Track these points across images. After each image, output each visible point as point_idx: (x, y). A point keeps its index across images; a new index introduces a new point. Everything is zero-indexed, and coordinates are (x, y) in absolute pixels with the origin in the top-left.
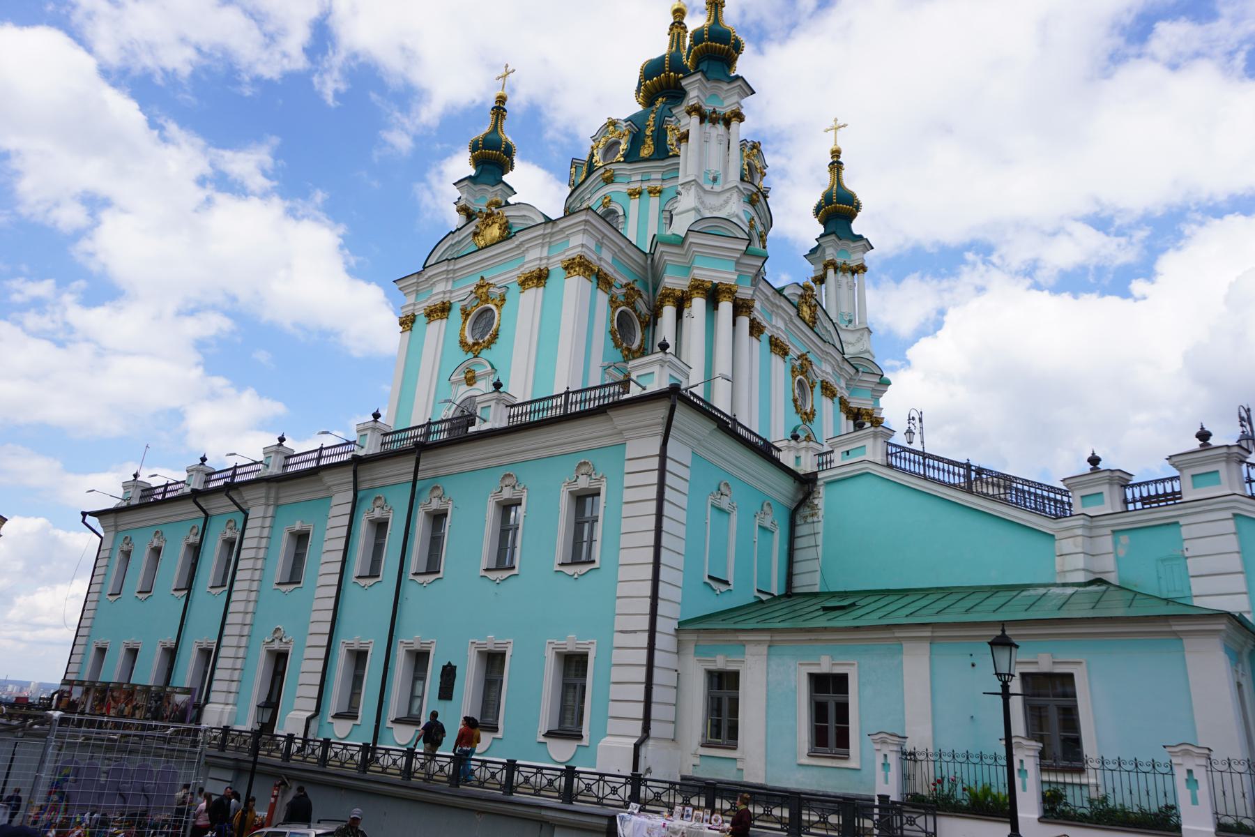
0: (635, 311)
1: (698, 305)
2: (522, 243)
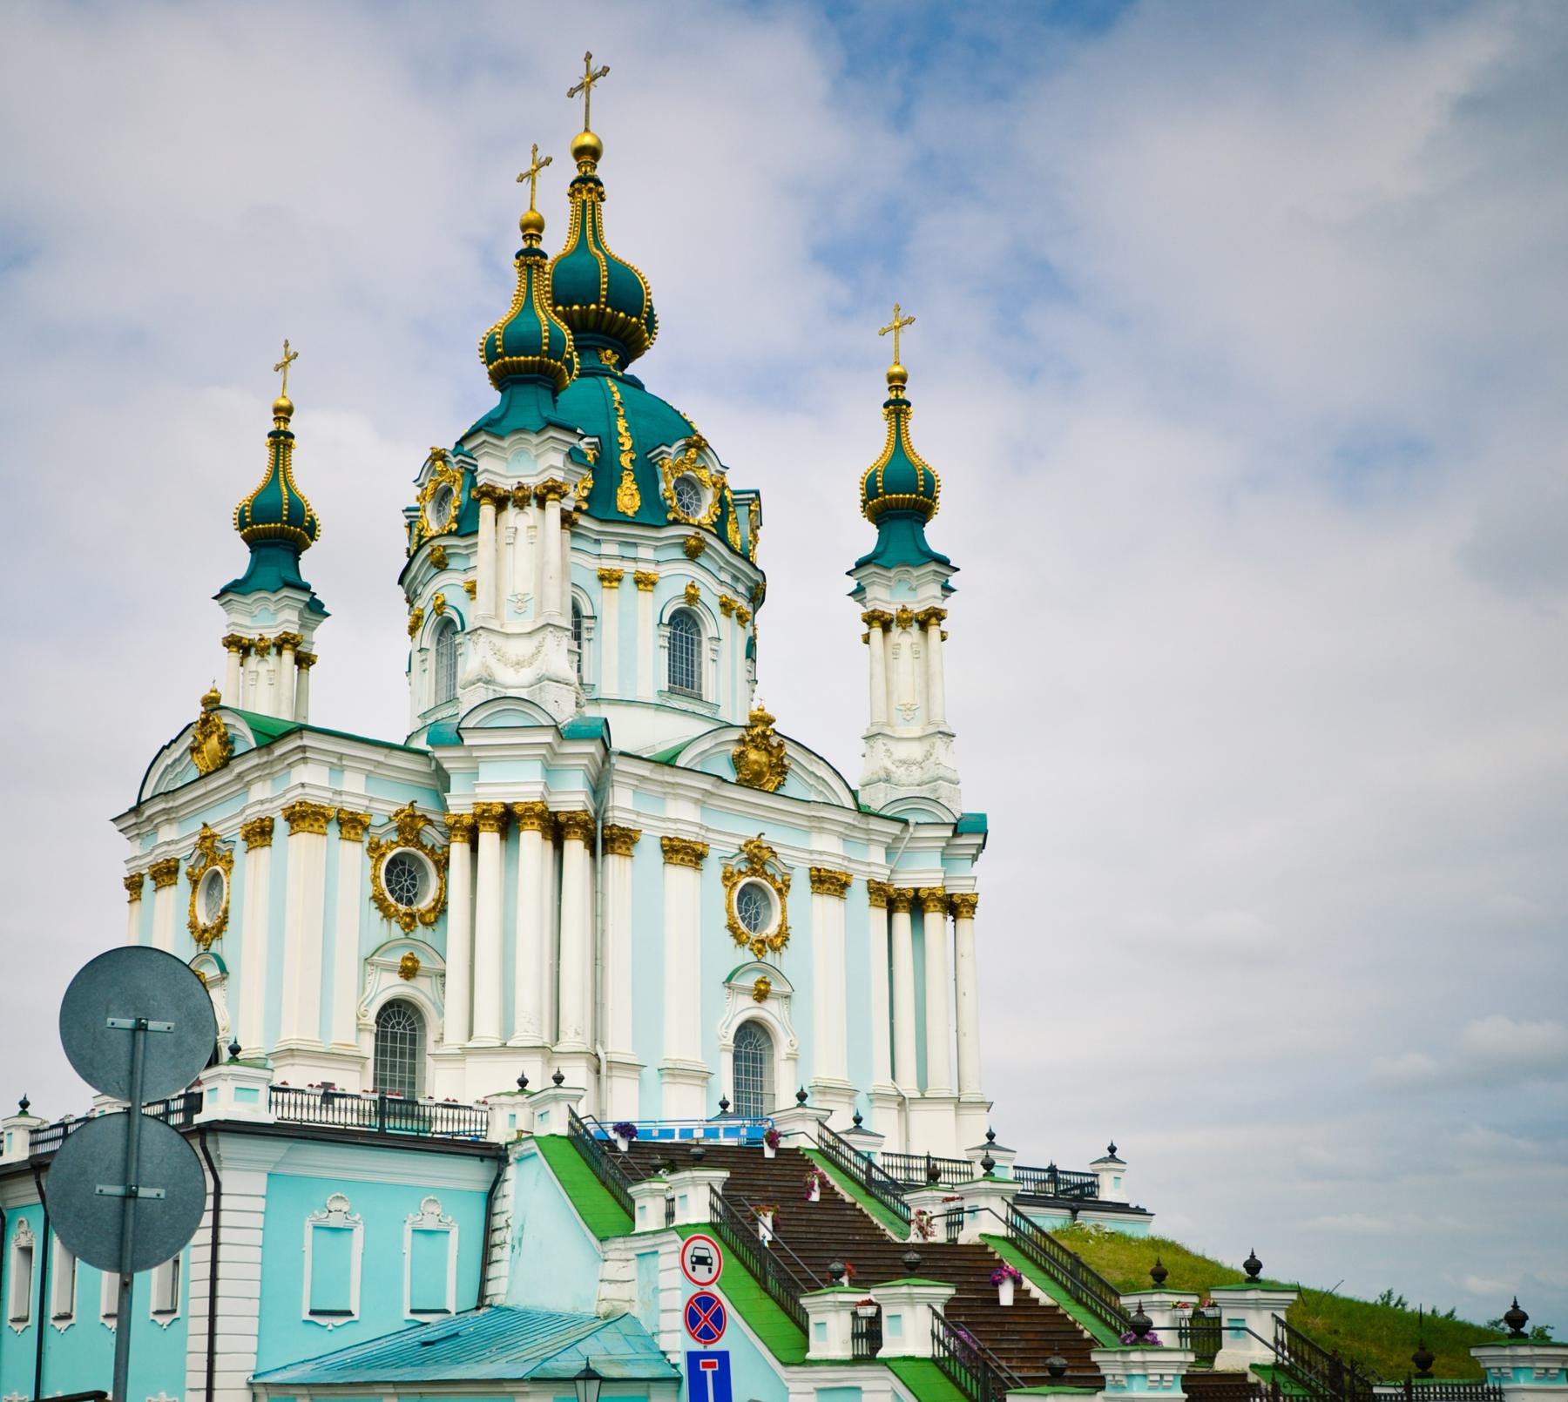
0: (423, 847)
1: (489, 840)
2: (240, 776)
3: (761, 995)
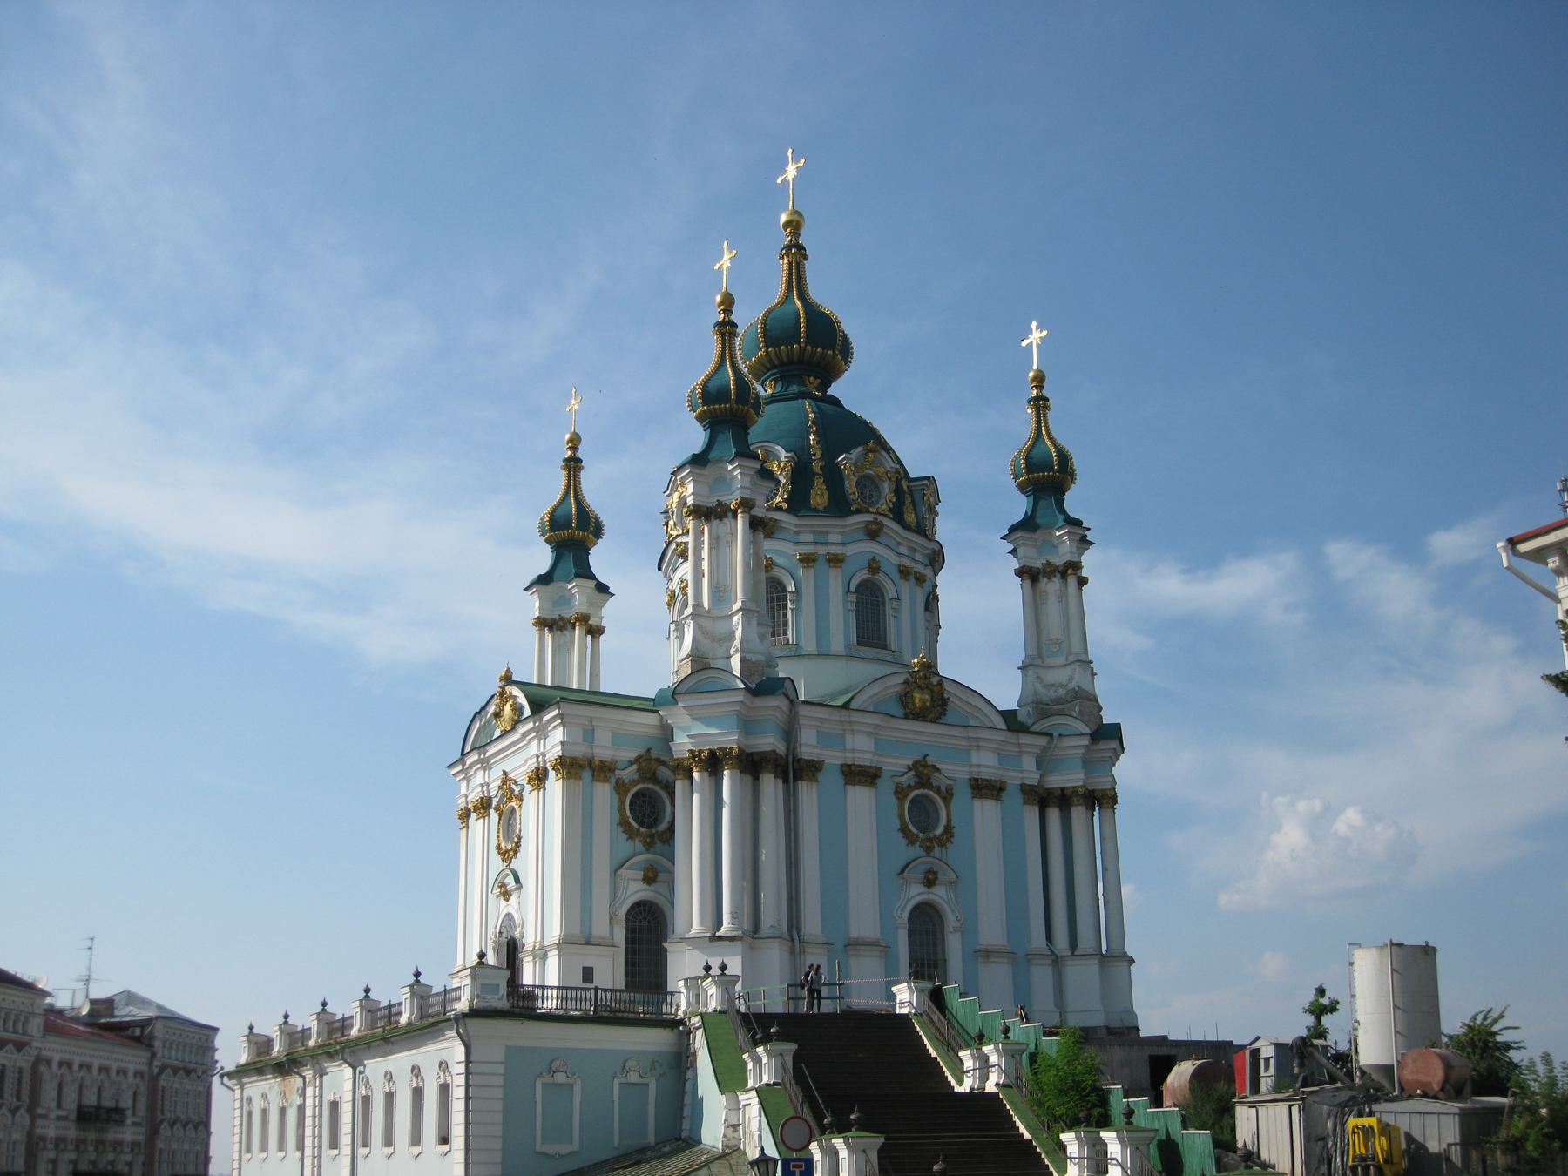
2: (524, 735)
3: (930, 880)
